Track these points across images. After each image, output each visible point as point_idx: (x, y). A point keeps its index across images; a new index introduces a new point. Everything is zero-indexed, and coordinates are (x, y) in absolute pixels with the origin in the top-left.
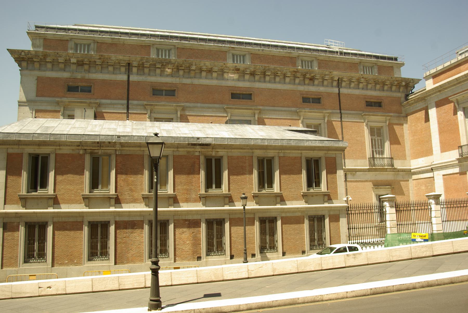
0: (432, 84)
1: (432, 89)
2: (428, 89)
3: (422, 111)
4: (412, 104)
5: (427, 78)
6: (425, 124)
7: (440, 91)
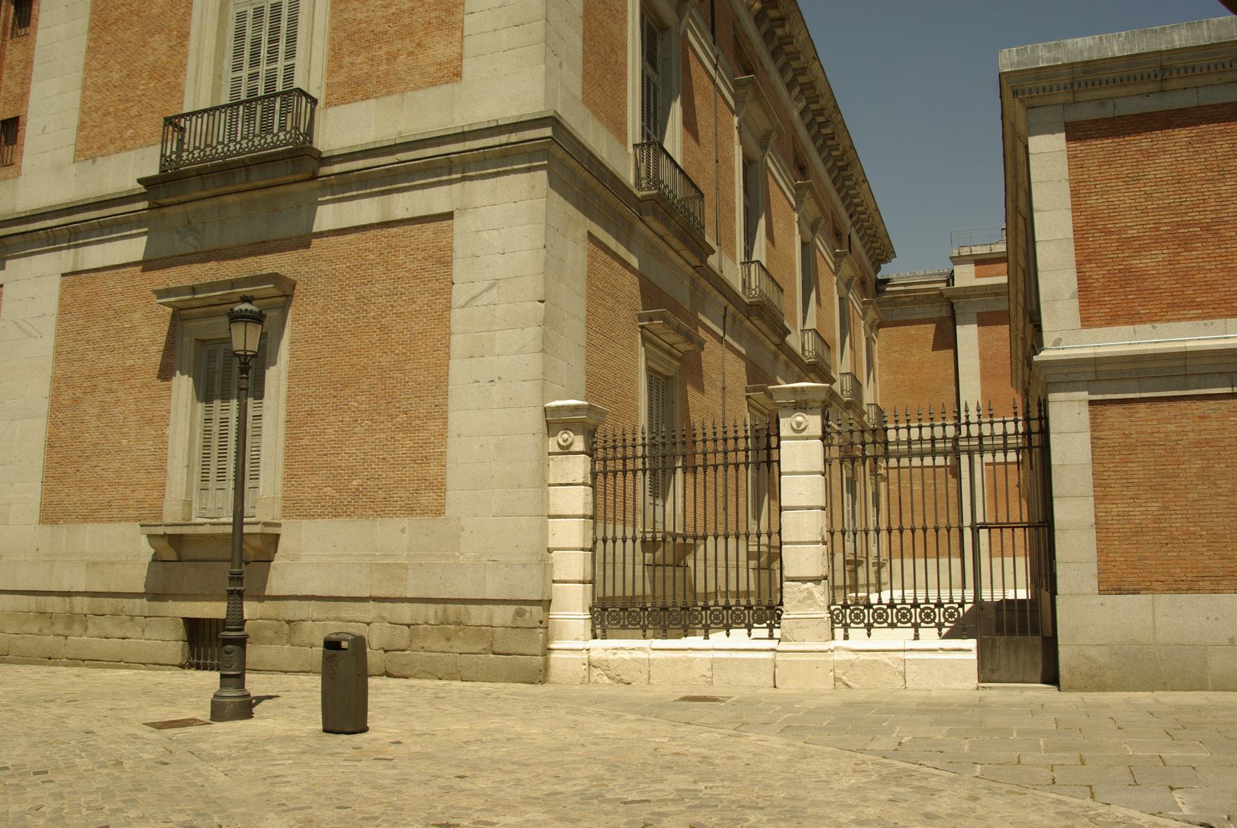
0: (974, 275)
1: (986, 286)
2: (959, 283)
3: (927, 325)
4: (905, 303)
5: (958, 260)
6: (935, 353)
7: (997, 294)
